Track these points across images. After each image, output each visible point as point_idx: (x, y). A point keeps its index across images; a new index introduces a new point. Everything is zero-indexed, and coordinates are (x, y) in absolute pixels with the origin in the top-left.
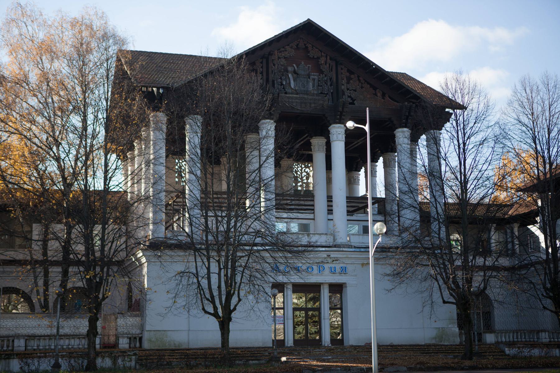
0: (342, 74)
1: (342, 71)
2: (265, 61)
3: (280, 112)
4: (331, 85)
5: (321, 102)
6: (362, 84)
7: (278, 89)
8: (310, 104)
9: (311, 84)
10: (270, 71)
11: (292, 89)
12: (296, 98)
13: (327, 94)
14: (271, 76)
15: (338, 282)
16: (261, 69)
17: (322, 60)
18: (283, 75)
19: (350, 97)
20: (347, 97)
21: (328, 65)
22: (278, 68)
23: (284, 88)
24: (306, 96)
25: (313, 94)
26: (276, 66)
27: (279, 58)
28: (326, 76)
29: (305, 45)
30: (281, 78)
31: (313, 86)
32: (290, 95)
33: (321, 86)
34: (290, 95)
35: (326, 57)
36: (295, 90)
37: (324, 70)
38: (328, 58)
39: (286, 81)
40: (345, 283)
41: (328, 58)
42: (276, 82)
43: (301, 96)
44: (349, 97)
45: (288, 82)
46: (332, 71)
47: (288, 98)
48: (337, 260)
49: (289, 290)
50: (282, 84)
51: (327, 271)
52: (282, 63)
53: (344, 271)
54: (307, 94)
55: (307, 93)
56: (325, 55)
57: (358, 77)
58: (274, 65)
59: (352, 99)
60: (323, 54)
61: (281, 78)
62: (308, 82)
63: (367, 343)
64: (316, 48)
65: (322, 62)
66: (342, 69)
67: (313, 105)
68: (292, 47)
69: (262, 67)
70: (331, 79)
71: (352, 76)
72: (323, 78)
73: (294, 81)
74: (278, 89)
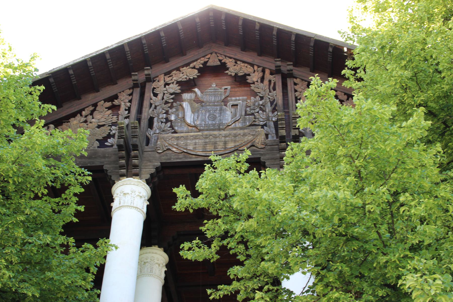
0: (296, 91)
1: (296, 87)
2: (137, 91)
3: (158, 164)
4: (274, 110)
5: (250, 138)
7: (160, 128)
9: (228, 113)
10: (146, 103)
12: (195, 138)
13: (265, 125)
14: (146, 113)
16: (128, 104)
17: (255, 77)
18: (171, 107)
21: (266, 82)
22: (163, 99)
23: (171, 127)
24: (216, 133)
26: (160, 96)
27: (166, 84)
28: (262, 98)
29: (220, 61)
30: (167, 113)
32: (182, 135)
33: (253, 114)
34: (182, 135)
35: (263, 71)
36: (195, 127)
37: (256, 90)
38: (267, 72)
42: (155, 119)
43: (206, 133)
45: (180, 116)
46: (274, 89)
47: (178, 138)
50: (167, 120)
52: (172, 91)
54: (219, 129)
56: (260, 69)
58: (156, 95)
60: (256, 67)
61: (167, 113)
64: (244, 62)
65: (255, 80)
66: (295, 84)
68: (194, 68)
69: (130, 101)
72: (255, 101)
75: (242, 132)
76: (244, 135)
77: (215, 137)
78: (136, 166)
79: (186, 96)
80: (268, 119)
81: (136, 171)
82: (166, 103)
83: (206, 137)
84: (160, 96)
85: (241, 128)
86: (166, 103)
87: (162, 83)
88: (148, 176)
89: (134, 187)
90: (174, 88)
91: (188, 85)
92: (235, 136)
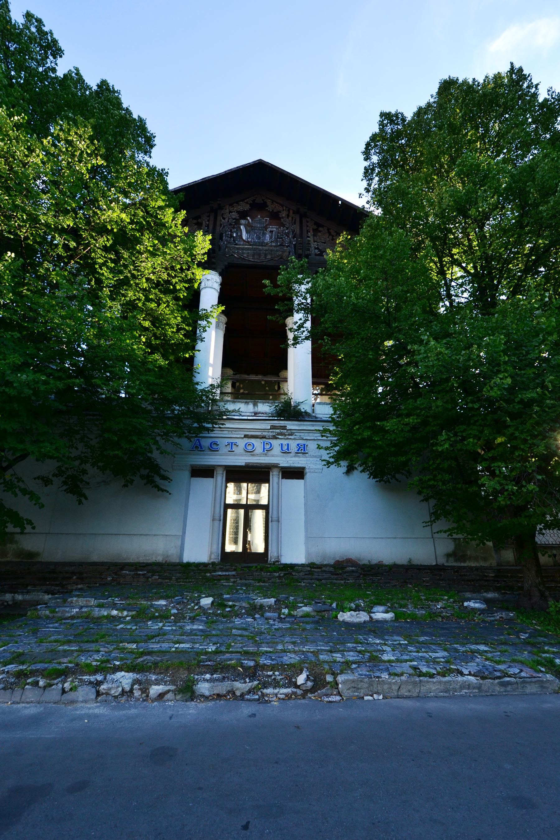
1: (308, 224)
3: (226, 263)
6: (333, 236)
7: (227, 241)
8: (266, 255)
10: (218, 223)
11: (244, 241)
12: (248, 249)
15: (292, 465)
17: (284, 214)
18: (234, 228)
19: (317, 248)
20: (313, 248)
21: (290, 218)
24: (260, 247)
25: (271, 246)
26: (226, 220)
27: (230, 212)
30: (231, 231)
31: (271, 238)
35: (289, 211)
36: (248, 242)
37: (285, 223)
38: (291, 211)
39: (237, 234)
40: (304, 468)
41: (291, 211)
44: (315, 248)
46: (295, 223)
47: (238, 249)
48: (291, 435)
49: (275, 476)
50: (232, 236)
51: (277, 450)
52: (234, 217)
53: (302, 450)
54: (262, 246)
55: (262, 244)
57: (328, 229)
58: (224, 219)
59: (320, 250)
61: (231, 231)
62: (264, 234)
63: (338, 561)
64: (277, 203)
66: (307, 222)
67: (269, 257)
68: (247, 203)
69: (208, 221)
70: (293, 232)
71: (320, 229)
73: (247, 232)
74: (227, 241)
75: (275, 249)
76: (277, 251)
77: (260, 250)
78: (214, 263)
79: (243, 221)
80: (290, 242)
81: (214, 266)
82: (231, 224)
83: (255, 249)
84: (226, 220)
85: (275, 246)
86: (231, 224)
87: (228, 210)
88: (221, 270)
89: (213, 277)
90: (235, 215)
91: (243, 215)
92: (271, 250)
